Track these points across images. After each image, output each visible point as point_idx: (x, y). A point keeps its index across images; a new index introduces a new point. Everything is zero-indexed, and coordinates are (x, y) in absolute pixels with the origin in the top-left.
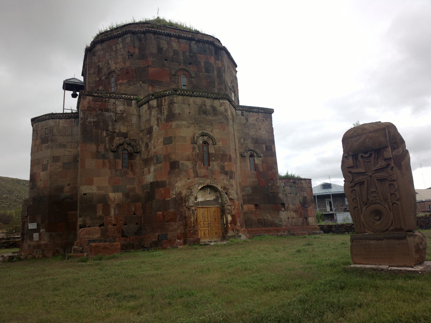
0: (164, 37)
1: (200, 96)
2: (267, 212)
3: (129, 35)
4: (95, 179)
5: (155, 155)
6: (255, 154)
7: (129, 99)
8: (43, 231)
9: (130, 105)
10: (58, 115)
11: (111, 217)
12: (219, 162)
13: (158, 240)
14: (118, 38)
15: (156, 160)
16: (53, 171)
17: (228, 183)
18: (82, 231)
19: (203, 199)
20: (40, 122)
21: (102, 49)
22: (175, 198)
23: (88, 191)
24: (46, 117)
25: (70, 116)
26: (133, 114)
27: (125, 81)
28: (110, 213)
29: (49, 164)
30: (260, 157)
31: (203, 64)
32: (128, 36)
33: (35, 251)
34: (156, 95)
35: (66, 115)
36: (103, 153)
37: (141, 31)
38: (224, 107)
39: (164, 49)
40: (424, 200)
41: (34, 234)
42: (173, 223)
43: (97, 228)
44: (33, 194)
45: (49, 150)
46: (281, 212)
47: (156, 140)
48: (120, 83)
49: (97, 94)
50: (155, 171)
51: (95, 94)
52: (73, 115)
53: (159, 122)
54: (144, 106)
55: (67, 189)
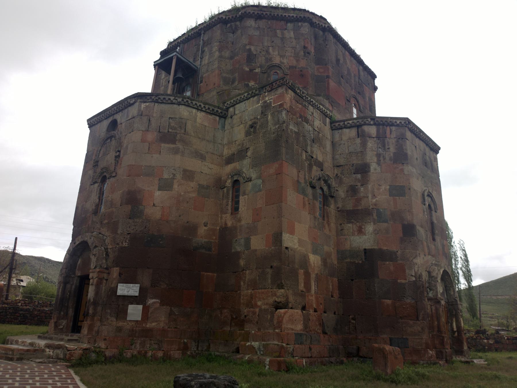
3: (306, 24)
5: (375, 207)
8: (154, 303)
10: (197, 103)
14: (287, 23)
16: (182, 194)
20: (156, 104)
21: (258, 28)
22: (414, 281)
23: (290, 245)
25: (215, 111)
28: (311, 287)
29: (175, 181)
33: (139, 342)
35: (209, 107)
42: (411, 322)
43: (299, 311)
45: (178, 157)
50: (376, 232)
52: (220, 111)
53: (380, 161)
55: (202, 230)
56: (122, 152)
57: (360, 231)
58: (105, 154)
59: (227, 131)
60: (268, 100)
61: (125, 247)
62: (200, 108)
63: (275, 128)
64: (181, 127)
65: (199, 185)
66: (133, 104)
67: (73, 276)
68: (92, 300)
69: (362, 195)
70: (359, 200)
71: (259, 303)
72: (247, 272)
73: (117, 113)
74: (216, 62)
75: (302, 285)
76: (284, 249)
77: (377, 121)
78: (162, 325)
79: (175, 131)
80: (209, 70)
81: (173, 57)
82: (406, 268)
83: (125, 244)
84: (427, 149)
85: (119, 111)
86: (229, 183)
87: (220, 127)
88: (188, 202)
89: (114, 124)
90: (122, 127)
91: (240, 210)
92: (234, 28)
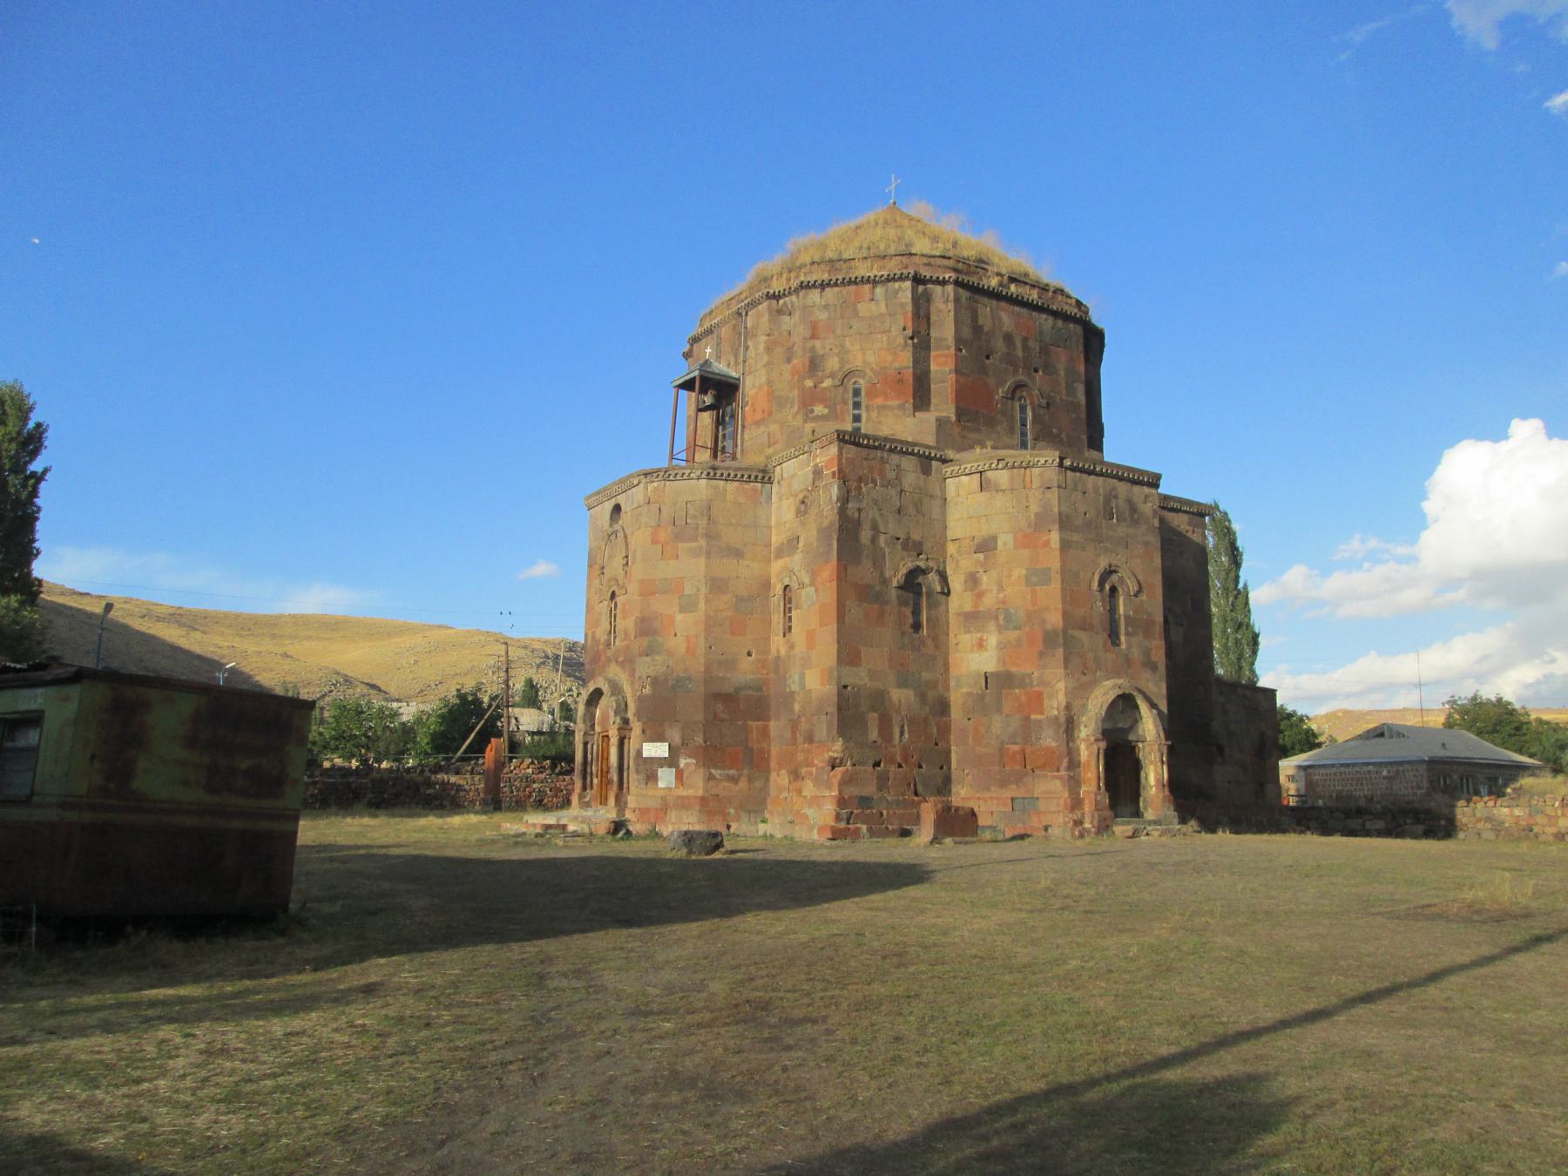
1: (1109, 476)
5: (1002, 606)
7: (929, 458)
8: (686, 764)
9: (926, 471)
11: (894, 746)
12: (1141, 638)
14: (874, 287)
17: (1156, 690)
20: (668, 483)
26: (931, 496)
27: (895, 403)
31: (1062, 373)
36: (878, 588)
38: (1150, 504)
39: (986, 329)
50: (1002, 646)
57: (981, 645)
58: (610, 558)
64: (702, 515)
69: (984, 587)
70: (980, 596)
71: (816, 762)
72: (803, 719)
74: (764, 372)
78: (701, 793)
81: (694, 378)
82: (1045, 696)
83: (648, 690)
84: (1122, 488)
86: (779, 590)
87: (763, 499)
90: (626, 517)
92: (789, 306)
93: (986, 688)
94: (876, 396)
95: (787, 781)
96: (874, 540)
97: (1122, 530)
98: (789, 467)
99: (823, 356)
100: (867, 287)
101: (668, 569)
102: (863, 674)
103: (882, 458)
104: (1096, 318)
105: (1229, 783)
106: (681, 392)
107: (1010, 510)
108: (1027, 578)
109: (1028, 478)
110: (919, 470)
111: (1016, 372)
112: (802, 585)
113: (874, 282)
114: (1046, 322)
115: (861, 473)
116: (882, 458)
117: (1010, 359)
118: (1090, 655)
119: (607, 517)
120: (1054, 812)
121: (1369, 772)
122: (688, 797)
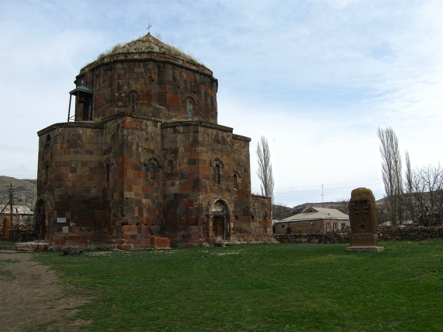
0: (178, 68)
1: (216, 129)
2: (243, 222)
3: (151, 62)
4: (134, 186)
5: (180, 171)
6: (237, 175)
7: (156, 121)
8: (73, 225)
9: (156, 126)
10: (86, 125)
11: (144, 218)
13: (183, 238)
15: (181, 176)
16: (82, 174)
17: (230, 199)
18: (126, 227)
19: (215, 210)
21: (123, 69)
23: (129, 196)
24: (75, 125)
27: (146, 102)
30: (241, 177)
31: (203, 94)
32: (150, 63)
34: (184, 123)
37: (162, 60)
39: (178, 78)
40: (323, 218)
41: (63, 227)
43: (135, 226)
44: (61, 192)
46: (251, 223)
47: (182, 160)
48: (140, 103)
49: (135, 116)
51: (134, 116)
54: (169, 129)
56: (53, 154)
57: (173, 184)
58: (46, 154)
59: (104, 137)
60: (119, 122)
61: (58, 201)
62: (88, 127)
63: (121, 138)
65: (90, 168)
66: (56, 128)
67: (39, 214)
68: (47, 225)
69: (174, 165)
70: (173, 168)
71: (117, 223)
72: (113, 210)
73: (50, 131)
74: (102, 90)
75: (137, 214)
76: (125, 199)
77: (183, 124)
78: (77, 235)
79: (76, 142)
80: (99, 94)
81: (77, 91)
82: (194, 201)
83: (58, 200)
84: (220, 133)
85: (51, 131)
86: (105, 165)
87: (100, 134)
88: (85, 178)
89: (49, 138)
90: (52, 140)
91: (110, 179)
93: (175, 198)
94: (140, 100)
95: (107, 231)
96: (137, 149)
97: (220, 146)
98: (109, 124)
99: (122, 85)
100: (137, 63)
101: (67, 158)
102: (133, 194)
103: (141, 121)
104: (215, 76)
105: (255, 228)
106: (72, 96)
107: (183, 139)
108: (188, 162)
109: (189, 129)
110: (153, 126)
111: (187, 93)
112: (113, 164)
113: (140, 61)
114: (198, 77)
115: (133, 126)
116: (141, 121)
117: (185, 89)
118: (209, 187)
119: (45, 139)
120: (196, 239)
121: (307, 223)
122: (73, 236)
